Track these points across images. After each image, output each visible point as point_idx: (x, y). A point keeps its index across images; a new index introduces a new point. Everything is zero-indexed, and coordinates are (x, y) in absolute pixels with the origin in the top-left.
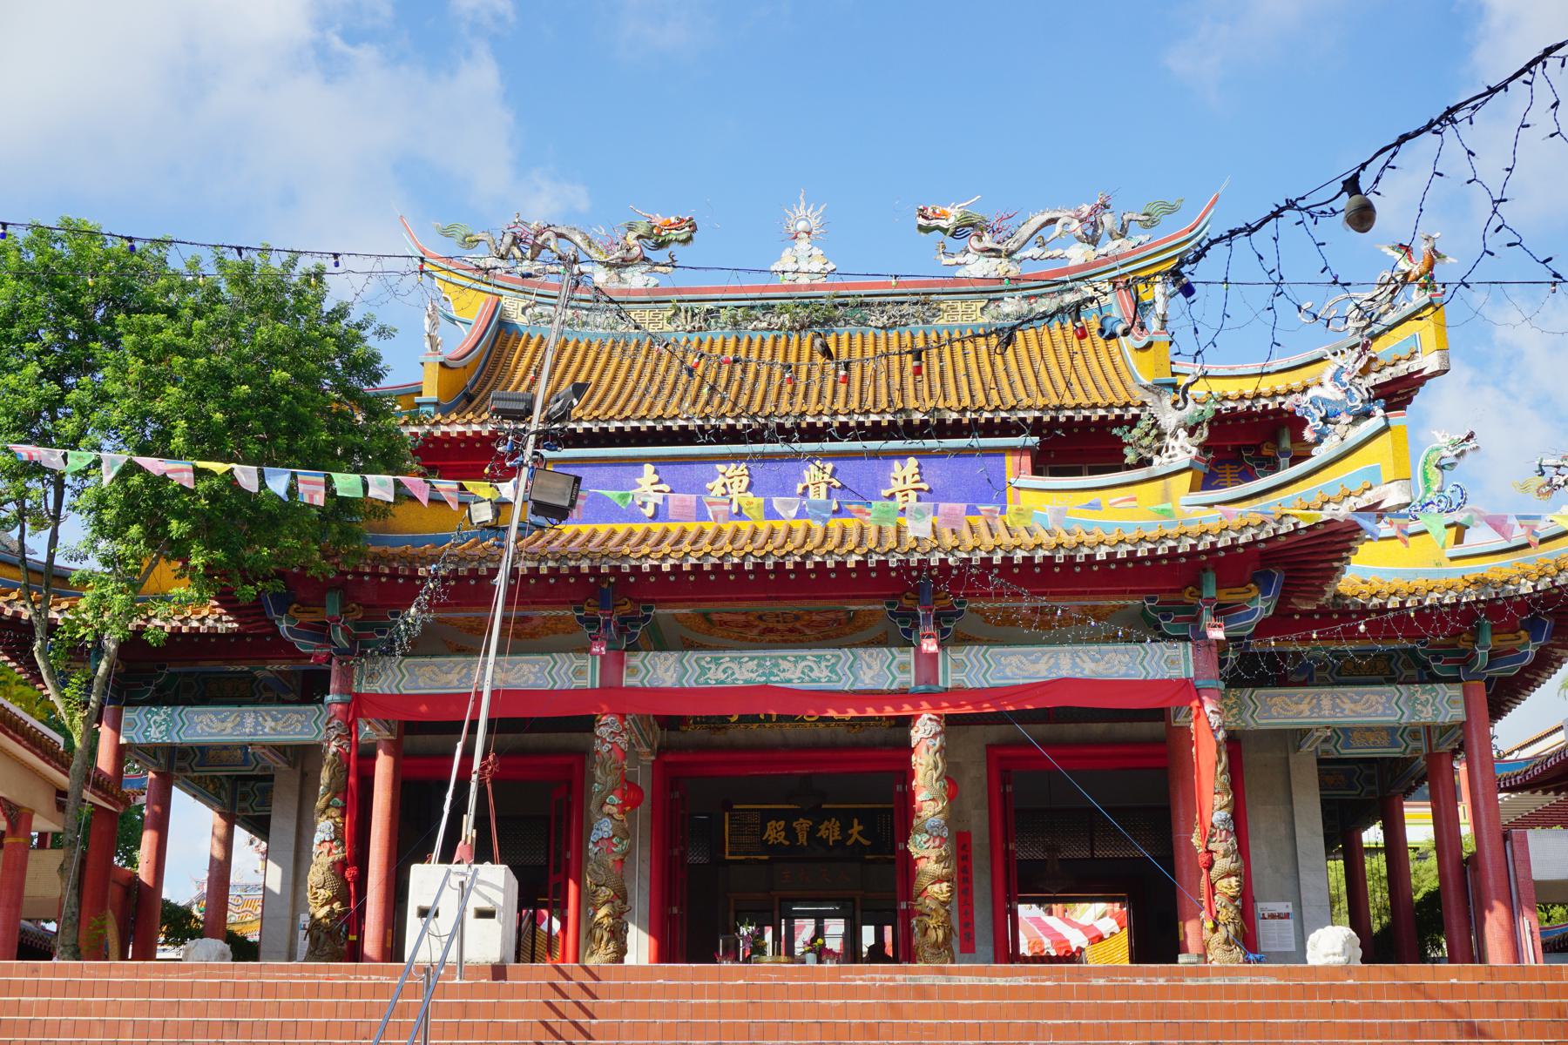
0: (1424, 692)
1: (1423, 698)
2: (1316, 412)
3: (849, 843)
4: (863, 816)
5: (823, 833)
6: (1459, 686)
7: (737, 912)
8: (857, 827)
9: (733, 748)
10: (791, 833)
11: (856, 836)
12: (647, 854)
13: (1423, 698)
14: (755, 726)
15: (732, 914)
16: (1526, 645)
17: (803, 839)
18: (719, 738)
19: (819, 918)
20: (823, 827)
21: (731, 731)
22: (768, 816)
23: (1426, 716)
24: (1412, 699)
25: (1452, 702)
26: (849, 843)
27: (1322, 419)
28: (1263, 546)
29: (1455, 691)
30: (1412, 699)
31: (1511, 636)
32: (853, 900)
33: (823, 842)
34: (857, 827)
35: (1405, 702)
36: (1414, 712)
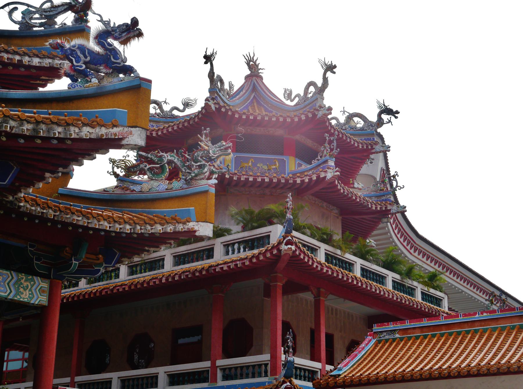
0: (26, 281)
1: (25, 284)
2: (81, 56)
6: (48, 281)
13: (25, 284)
16: (100, 265)
23: (25, 297)
24: (18, 283)
25: (42, 291)
27: (85, 63)
28: (39, 141)
29: (45, 285)
30: (18, 283)
31: (94, 257)
35: (14, 284)
36: (18, 293)
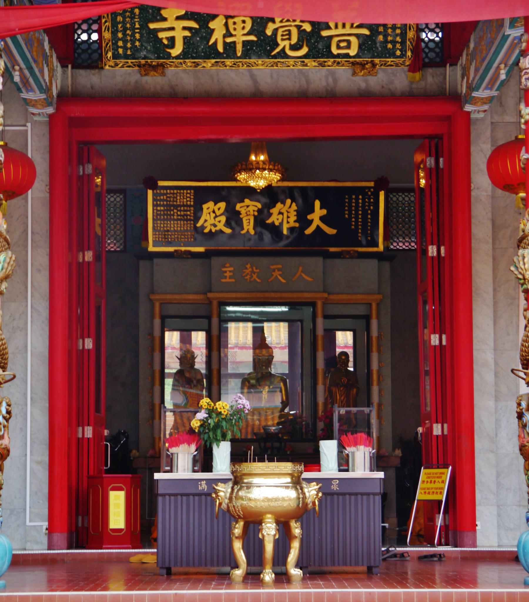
3: (309, 231)
4: (321, 194)
5: (275, 219)
7: (163, 318)
8: (318, 212)
9: (175, 97)
10: (233, 218)
11: (317, 222)
12: (45, 260)
14: (209, 64)
15: (157, 322)
17: (248, 226)
18: (153, 82)
19: (258, 321)
20: (275, 211)
21: (171, 71)
22: (202, 196)
26: (309, 231)
32: (313, 304)
33: (276, 230)
34: (318, 212)
